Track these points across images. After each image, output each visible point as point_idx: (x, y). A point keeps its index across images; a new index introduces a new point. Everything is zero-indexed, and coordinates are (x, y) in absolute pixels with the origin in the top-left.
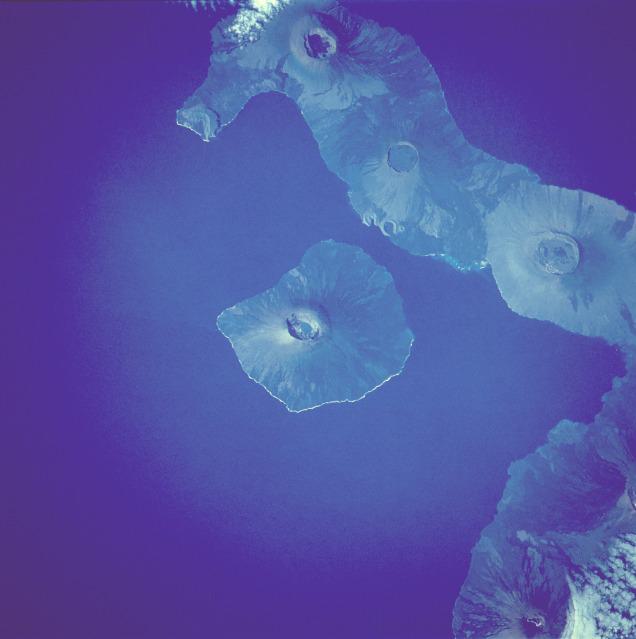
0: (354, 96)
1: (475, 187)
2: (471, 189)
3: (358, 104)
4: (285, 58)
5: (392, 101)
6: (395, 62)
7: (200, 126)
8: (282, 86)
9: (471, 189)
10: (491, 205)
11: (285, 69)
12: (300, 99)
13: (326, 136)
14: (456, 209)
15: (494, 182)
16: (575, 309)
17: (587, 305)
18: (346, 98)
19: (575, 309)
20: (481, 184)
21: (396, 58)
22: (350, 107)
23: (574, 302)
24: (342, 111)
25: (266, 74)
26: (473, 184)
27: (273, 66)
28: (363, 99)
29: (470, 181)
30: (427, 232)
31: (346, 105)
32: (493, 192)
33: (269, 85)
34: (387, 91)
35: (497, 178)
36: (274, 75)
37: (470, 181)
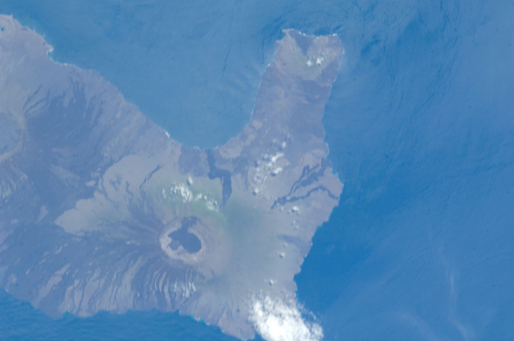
0: (104, 192)
3: (91, 183)
4: (224, 200)
5: (44, 211)
6: (63, 271)
7: (304, 45)
8: (211, 159)
11: (218, 183)
12: (178, 152)
13: (118, 115)
18: (113, 183)
21: (64, 276)
22: (102, 173)
24: (112, 163)
25: (242, 164)
27: (236, 181)
28: (89, 194)
31: (110, 174)
33: (231, 151)
34: (58, 222)
36: (229, 167)
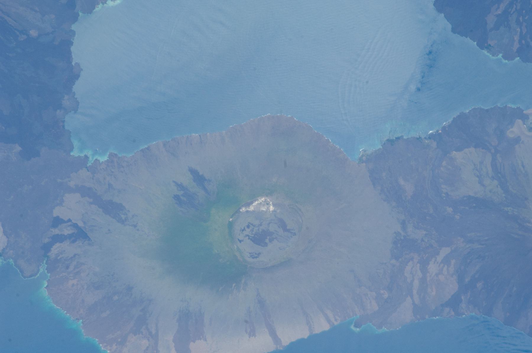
1: (440, 258)
2: (445, 251)
9: (445, 251)
10: (403, 246)
14: (450, 210)
15: (416, 283)
16: (193, 172)
17: (180, 186)
19: (193, 172)
20: (433, 268)
23: (199, 179)
26: (446, 261)
29: (453, 262)
30: (472, 149)
32: (410, 263)
35: (415, 292)
37: (453, 262)
